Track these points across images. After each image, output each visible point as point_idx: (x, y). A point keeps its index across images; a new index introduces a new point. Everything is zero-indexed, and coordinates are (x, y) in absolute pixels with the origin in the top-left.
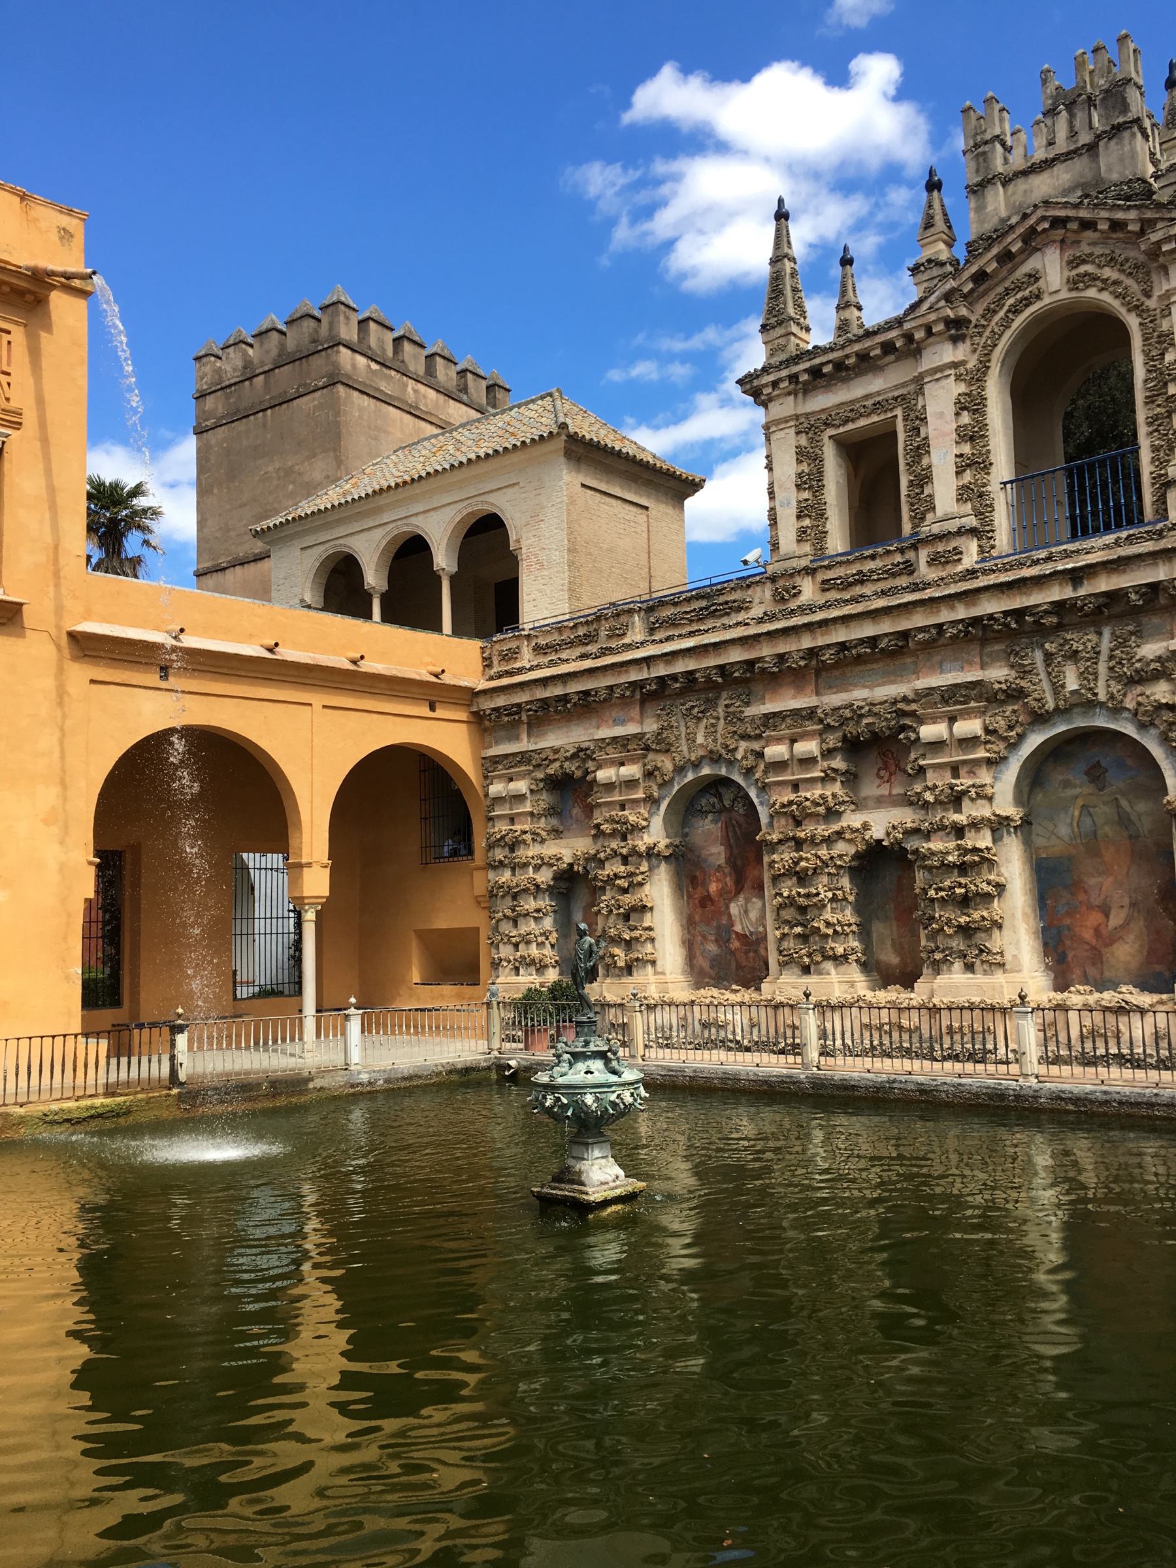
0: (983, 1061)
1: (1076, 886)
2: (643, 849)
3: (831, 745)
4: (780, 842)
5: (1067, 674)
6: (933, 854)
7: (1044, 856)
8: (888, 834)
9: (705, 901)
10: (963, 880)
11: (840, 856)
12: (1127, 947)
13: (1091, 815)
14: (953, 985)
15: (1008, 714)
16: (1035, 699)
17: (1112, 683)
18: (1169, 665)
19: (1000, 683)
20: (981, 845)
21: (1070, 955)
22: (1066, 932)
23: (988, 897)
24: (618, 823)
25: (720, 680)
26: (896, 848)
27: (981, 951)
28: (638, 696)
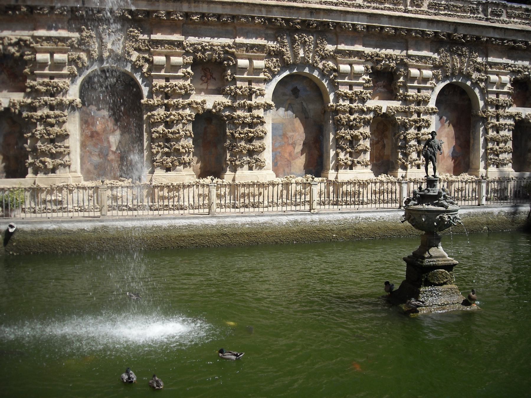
0: (258, 207)
2: (68, 103)
3: (189, 61)
4: (158, 106)
6: (239, 117)
8: (215, 107)
9: (94, 135)
11: (190, 115)
12: (300, 160)
13: (292, 108)
14: (244, 175)
17: (317, 57)
19: (273, 47)
20: (261, 115)
21: (279, 163)
24: (50, 86)
25: (130, 17)
28: (70, 16)
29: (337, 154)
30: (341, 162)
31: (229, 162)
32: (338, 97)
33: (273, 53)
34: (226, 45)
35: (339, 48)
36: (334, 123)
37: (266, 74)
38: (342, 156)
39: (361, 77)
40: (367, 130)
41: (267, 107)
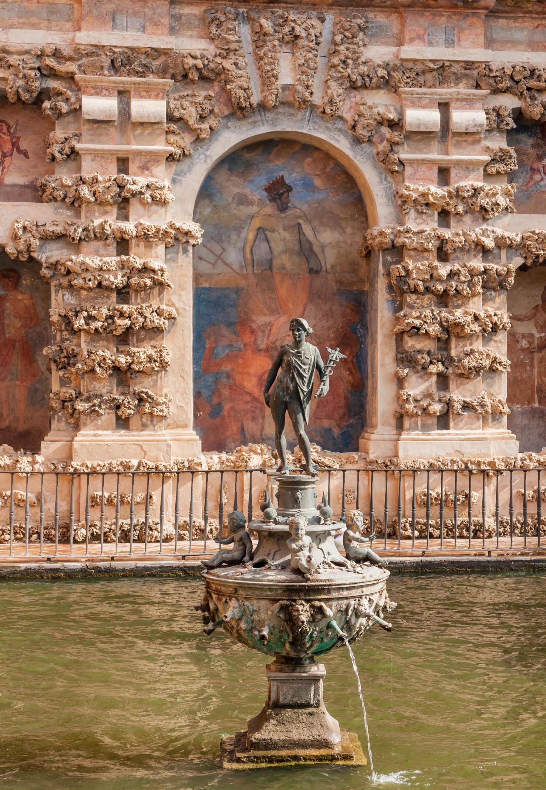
0: (140, 539)
1: (241, 324)
5: (281, 63)
7: (206, 285)
8: (16, 238)
10: (126, 308)
15: (200, 99)
16: (241, 88)
17: (333, 84)
18: (397, 75)
19: (194, 57)
20: (156, 264)
22: (225, 380)
23: (158, 331)
26: (24, 258)
27: (141, 400)
29: (400, 382)
30: (410, 407)
31: (55, 404)
32: (402, 203)
33: (194, 75)
34: (48, 51)
35: (403, 56)
36: (390, 287)
37: (172, 138)
38: (416, 387)
39: (479, 141)
40: (497, 309)
41: (177, 239)
